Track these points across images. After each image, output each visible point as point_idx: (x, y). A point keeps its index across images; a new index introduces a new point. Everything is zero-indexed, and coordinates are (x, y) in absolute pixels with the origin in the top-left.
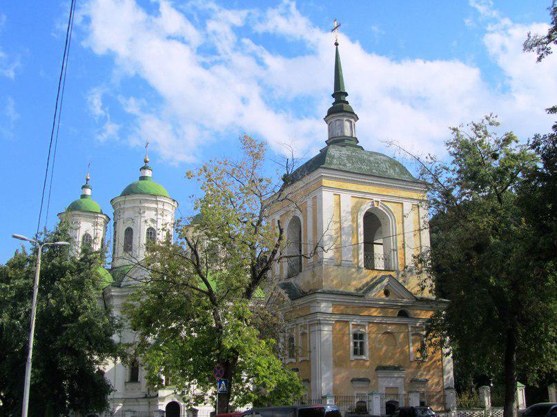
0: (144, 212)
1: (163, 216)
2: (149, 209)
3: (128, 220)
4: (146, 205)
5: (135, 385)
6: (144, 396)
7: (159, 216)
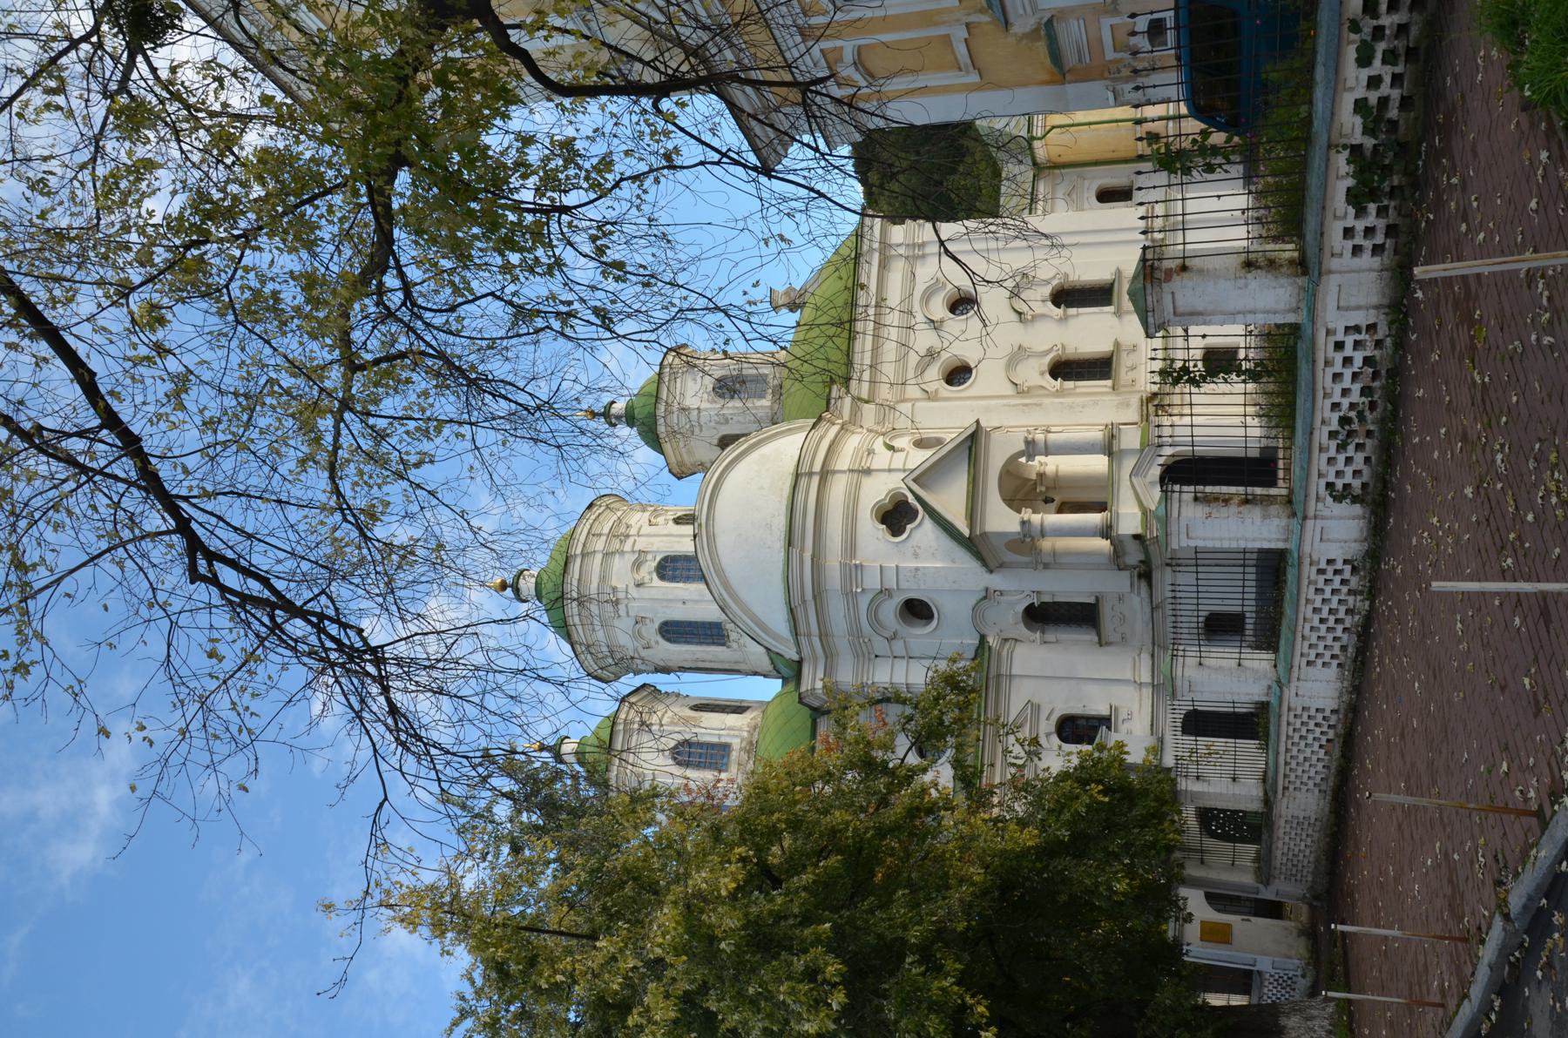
0: (614, 589)
1: (628, 536)
2: (603, 578)
3: (638, 635)
4: (594, 585)
5: (1107, 614)
6: (1143, 584)
7: (628, 547)
